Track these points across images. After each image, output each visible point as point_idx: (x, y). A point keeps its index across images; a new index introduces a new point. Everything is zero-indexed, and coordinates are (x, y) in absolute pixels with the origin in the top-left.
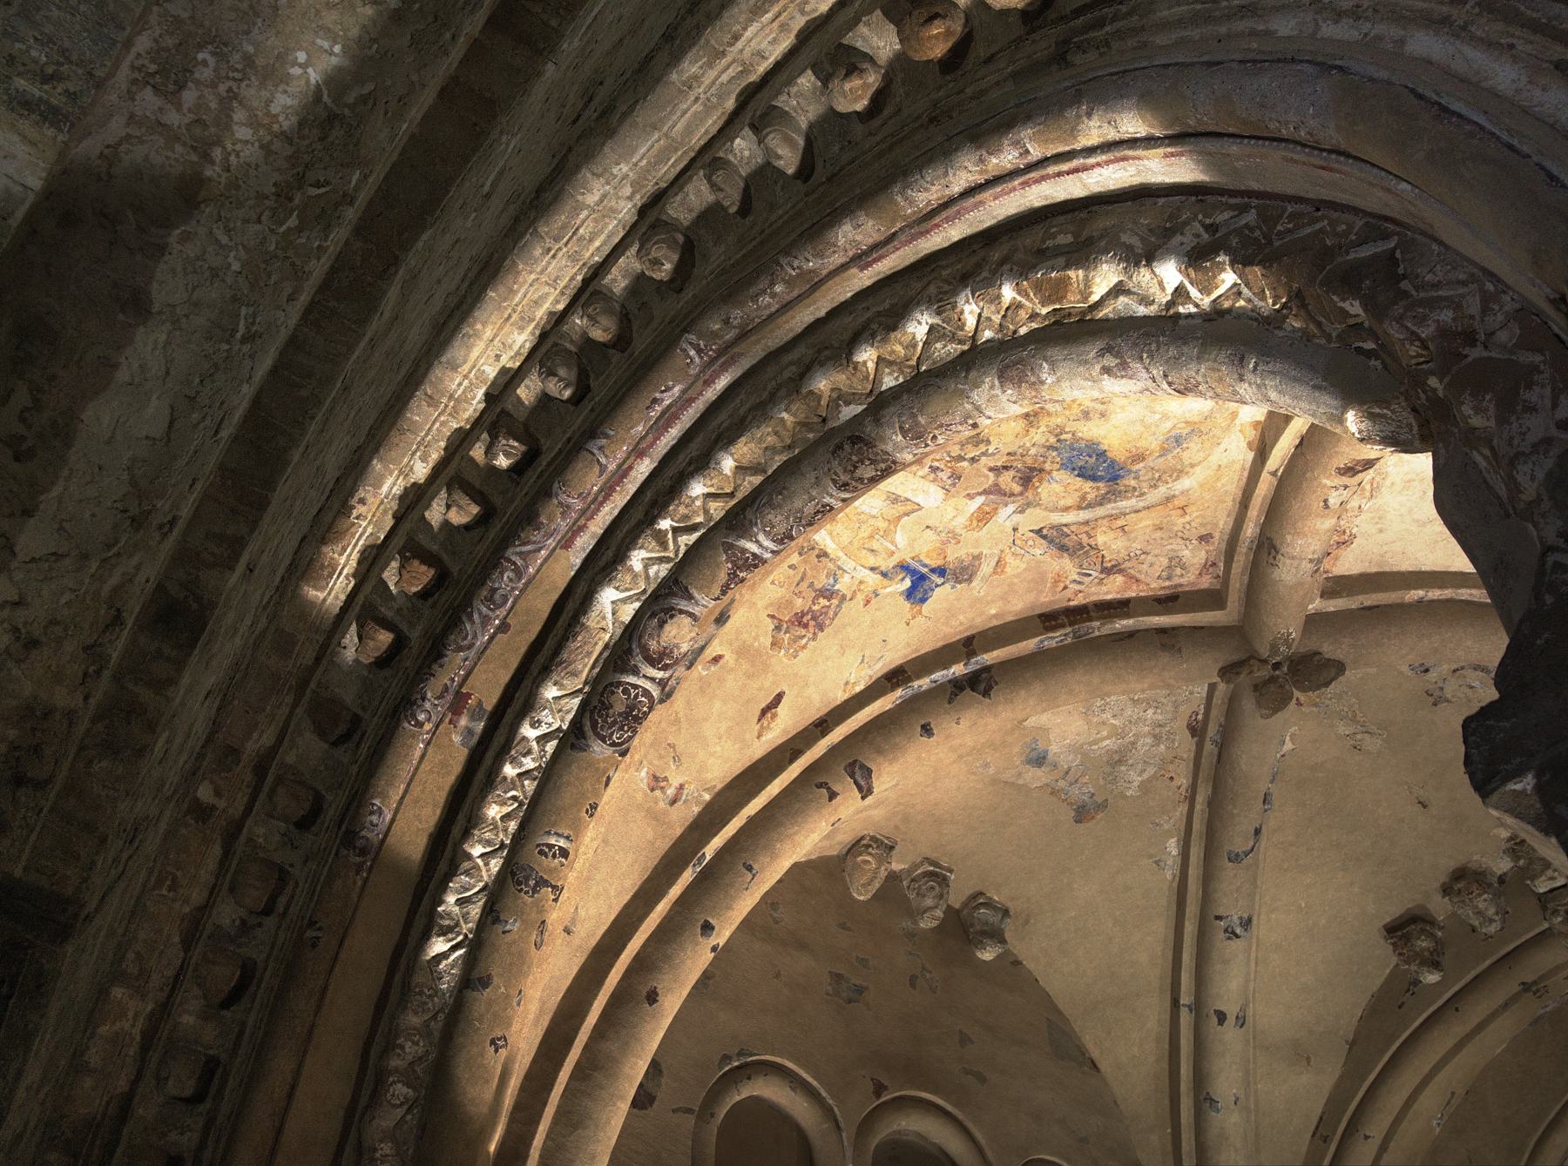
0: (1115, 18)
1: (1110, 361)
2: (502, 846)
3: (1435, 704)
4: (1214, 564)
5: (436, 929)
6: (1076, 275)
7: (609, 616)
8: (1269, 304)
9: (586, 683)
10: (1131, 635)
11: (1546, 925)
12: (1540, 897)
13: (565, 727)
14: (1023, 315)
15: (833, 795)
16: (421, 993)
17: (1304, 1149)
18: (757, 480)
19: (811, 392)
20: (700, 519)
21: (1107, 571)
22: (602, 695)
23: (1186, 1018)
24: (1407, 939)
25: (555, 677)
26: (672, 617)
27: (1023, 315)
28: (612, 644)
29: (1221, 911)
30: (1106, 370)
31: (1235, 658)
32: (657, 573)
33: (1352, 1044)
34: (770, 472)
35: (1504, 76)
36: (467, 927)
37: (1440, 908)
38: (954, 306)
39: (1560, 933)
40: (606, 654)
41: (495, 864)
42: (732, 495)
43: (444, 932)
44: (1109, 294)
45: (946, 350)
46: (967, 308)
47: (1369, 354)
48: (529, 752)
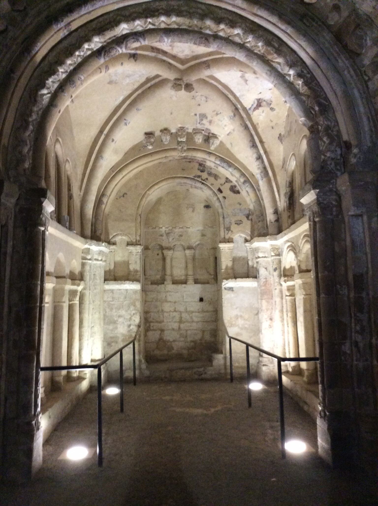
0: (317, 23)
1: (269, 73)
2: (66, 72)
3: (192, 99)
4: (188, 56)
5: (46, 87)
6: (275, 55)
7: (121, 30)
8: (301, 91)
9: (105, 42)
10: (164, 61)
11: (176, 147)
12: (178, 141)
13: (95, 49)
14: (258, 49)
15: (101, 72)
16: (39, 103)
17: (107, 172)
18: (176, 27)
19: (205, 23)
20: (157, 24)
21: (171, 46)
22: (110, 49)
23: (103, 137)
24: (150, 137)
25: (100, 37)
26: (138, 42)
27: (258, 49)
28: (117, 36)
29: (127, 119)
30: (267, 73)
31: (179, 78)
32: (138, 28)
33: (126, 154)
34: (181, 28)
35: (362, 109)
36: (53, 89)
37: (158, 133)
38: (248, 36)
39: (179, 150)
40: (114, 38)
41: (64, 76)
42: (168, 25)
43: (48, 88)
44: (277, 62)
45: (237, 40)
46: (249, 39)
47: (312, 113)
48: (83, 51)
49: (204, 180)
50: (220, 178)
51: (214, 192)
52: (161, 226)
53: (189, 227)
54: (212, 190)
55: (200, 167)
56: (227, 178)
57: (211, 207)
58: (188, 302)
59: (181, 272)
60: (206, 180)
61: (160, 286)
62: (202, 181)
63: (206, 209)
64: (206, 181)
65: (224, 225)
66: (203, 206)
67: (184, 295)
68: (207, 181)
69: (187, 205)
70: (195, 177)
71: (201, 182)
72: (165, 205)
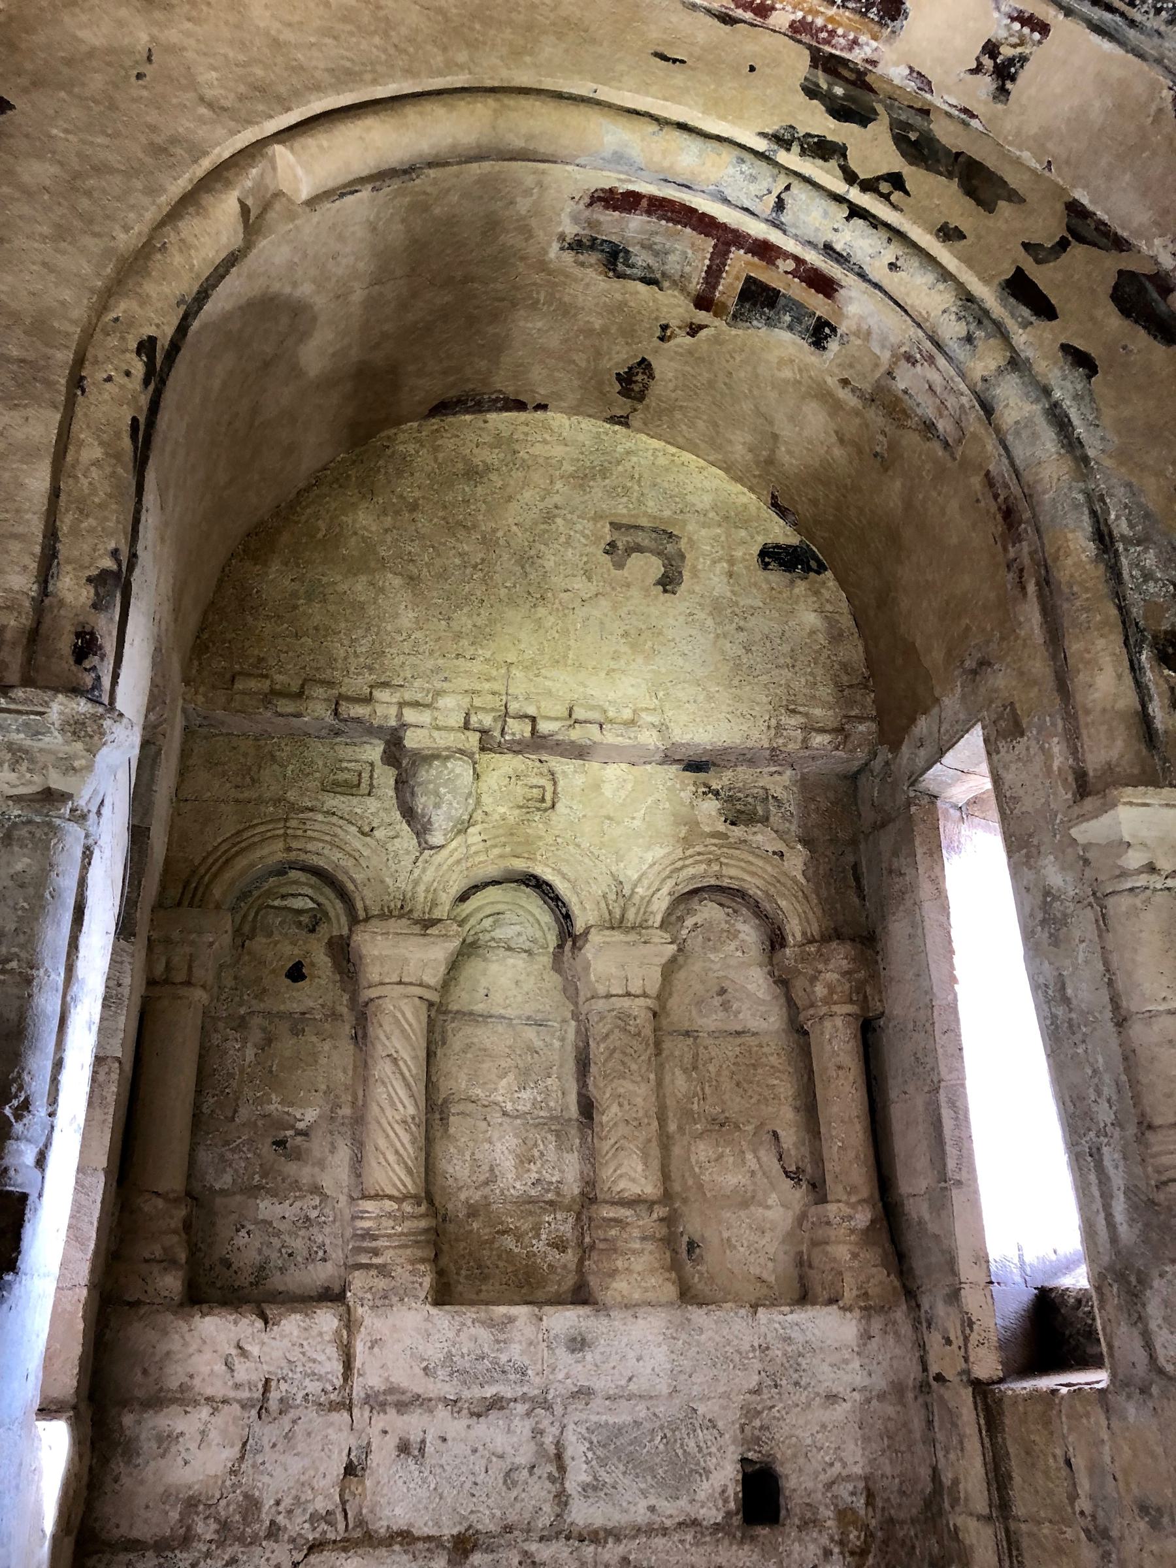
49: (868, 186)
50: (1014, 197)
51: (968, 298)
52: (358, 684)
53: (627, 714)
54: (946, 275)
55: (823, 82)
56: (1075, 210)
57: (821, 569)
58: (614, 1534)
59: (524, 1160)
60: (885, 187)
61: (291, 1324)
62: (855, 195)
63: (776, 577)
64: (886, 197)
65: (1123, 610)
66: (756, 550)
67: (575, 1449)
68: (896, 196)
69: (615, 526)
70: (782, 140)
71: (839, 199)
72: (414, 507)
